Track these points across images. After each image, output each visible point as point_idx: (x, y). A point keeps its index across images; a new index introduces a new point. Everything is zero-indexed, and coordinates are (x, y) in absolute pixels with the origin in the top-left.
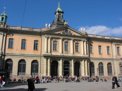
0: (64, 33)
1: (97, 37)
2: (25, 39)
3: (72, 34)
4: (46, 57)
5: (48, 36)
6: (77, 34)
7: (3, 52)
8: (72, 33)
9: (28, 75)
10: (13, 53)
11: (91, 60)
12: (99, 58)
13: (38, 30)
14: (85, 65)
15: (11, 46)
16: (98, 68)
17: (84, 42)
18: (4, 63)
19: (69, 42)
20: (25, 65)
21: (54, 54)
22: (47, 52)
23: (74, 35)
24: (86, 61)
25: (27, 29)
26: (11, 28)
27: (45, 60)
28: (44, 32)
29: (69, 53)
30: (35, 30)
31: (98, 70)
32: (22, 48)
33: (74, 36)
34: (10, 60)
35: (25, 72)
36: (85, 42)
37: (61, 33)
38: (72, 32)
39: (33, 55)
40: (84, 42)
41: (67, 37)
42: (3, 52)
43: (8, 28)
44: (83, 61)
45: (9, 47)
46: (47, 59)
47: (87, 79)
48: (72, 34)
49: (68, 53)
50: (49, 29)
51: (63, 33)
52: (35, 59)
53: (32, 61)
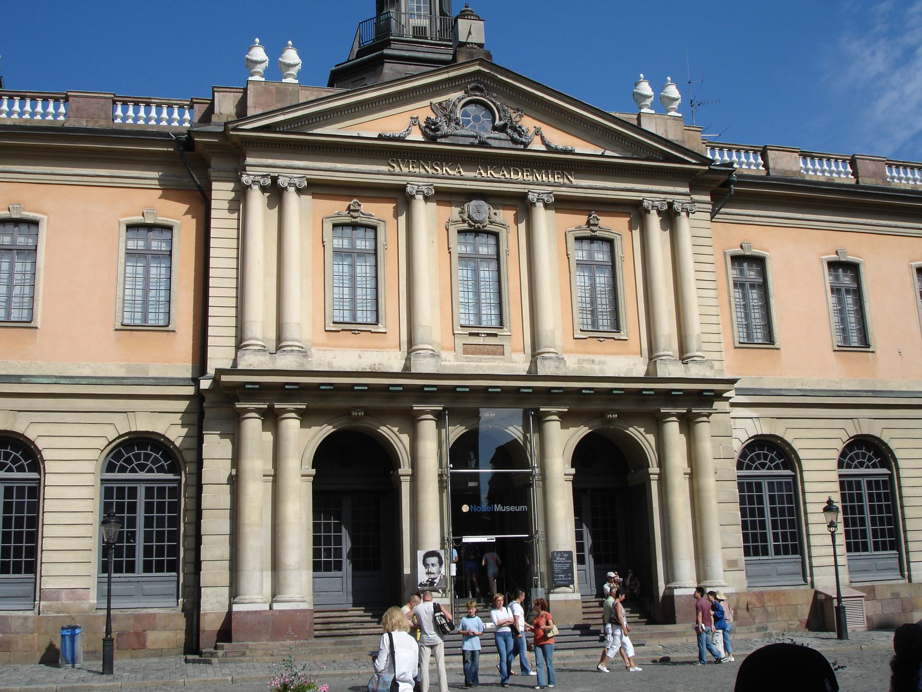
1: (811, 176)
5: (274, 172)
6: (583, 148)
8: (537, 132)
9: (65, 601)
12: (837, 393)
13: (178, 120)
14: (693, 476)
16: (837, 498)
20: (35, 491)
25: (52, 113)
28: (224, 135)
29: (507, 349)
30: (128, 117)
31: (833, 535)
35: (31, 568)
38: (528, 123)
40: (670, 217)
41: (484, 184)
48: (537, 145)
49: (499, 350)
50: (282, 92)
51: (431, 130)
53: (102, 443)
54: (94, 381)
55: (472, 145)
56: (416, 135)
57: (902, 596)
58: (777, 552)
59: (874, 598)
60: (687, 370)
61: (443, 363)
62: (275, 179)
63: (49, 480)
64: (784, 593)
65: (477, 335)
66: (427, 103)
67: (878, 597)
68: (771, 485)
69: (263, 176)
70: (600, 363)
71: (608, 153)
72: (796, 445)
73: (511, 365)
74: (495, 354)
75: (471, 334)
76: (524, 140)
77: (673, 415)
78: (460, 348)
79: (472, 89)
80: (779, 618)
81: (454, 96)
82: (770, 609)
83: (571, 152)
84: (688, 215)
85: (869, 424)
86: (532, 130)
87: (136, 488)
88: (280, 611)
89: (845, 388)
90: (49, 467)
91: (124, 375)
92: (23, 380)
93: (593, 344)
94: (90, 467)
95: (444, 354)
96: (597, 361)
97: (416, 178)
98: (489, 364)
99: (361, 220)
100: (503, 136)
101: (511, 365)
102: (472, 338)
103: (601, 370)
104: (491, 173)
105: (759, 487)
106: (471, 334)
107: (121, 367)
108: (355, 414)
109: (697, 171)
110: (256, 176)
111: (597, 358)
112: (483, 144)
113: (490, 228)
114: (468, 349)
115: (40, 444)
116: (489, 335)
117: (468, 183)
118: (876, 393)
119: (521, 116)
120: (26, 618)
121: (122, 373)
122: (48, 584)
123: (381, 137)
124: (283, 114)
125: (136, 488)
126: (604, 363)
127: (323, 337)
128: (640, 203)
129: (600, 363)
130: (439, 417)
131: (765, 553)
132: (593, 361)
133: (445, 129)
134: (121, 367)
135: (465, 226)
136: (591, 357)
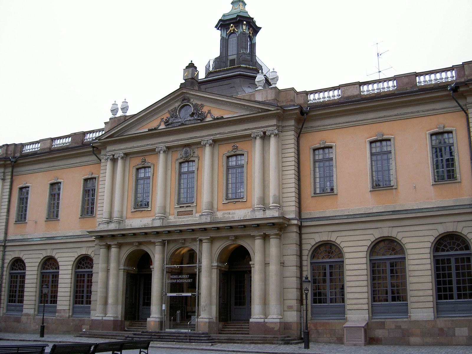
0: (172, 123)
2: (59, 180)
3: (209, 115)
4: (105, 239)
5: (113, 153)
8: (209, 112)
10: (26, 237)
15: (22, 217)
17: (265, 137)
19: (196, 160)
21: (137, 222)
23: (215, 119)
24: (273, 242)
27: (103, 251)
29: (194, 212)
33: (220, 123)
36: (273, 141)
39: (78, 236)
44: (258, 242)
47: (283, 335)
48: (209, 119)
49: (190, 213)
52: (84, 252)
53: (74, 259)
54: (72, 237)
55: (179, 126)
56: (163, 126)
57: (403, 327)
59: (384, 328)
60: (264, 214)
61: (169, 221)
62: (114, 155)
63: (61, 272)
64: (328, 323)
65: (183, 207)
66: (166, 111)
67: (386, 328)
69: (111, 155)
70: (232, 214)
72: (342, 245)
73: (195, 219)
74: (190, 215)
75: (180, 207)
76: (199, 118)
77: (257, 236)
78: (176, 214)
79: (183, 100)
80: (325, 336)
81: (177, 105)
82: (320, 331)
83: (222, 118)
84: (276, 135)
85: (385, 231)
86: (207, 112)
87: (85, 274)
88: (105, 320)
89: (375, 211)
90: (61, 268)
91: (81, 234)
92: (55, 238)
93: (231, 206)
94: (70, 267)
95: (170, 217)
96: (231, 213)
98: (187, 219)
99: (146, 165)
100: (192, 118)
101: (195, 219)
102: (181, 209)
103: (233, 217)
106: (180, 207)
107: (80, 231)
108: (135, 244)
109: (277, 113)
110: (109, 155)
111: (231, 211)
112: (183, 124)
113: (192, 159)
114: (179, 214)
115: (58, 260)
116: (187, 206)
117: (179, 142)
118: (394, 212)
119: (202, 106)
120: (53, 319)
121: (80, 234)
122: (59, 308)
123: (149, 130)
124: (114, 130)
125: (85, 274)
126: (234, 213)
127: (130, 215)
128: (249, 136)
129: (232, 214)
130: (163, 243)
132: (229, 213)
133: (170, 122)
134: (80, 231)
135: (181, 160)
136: (229, 211)
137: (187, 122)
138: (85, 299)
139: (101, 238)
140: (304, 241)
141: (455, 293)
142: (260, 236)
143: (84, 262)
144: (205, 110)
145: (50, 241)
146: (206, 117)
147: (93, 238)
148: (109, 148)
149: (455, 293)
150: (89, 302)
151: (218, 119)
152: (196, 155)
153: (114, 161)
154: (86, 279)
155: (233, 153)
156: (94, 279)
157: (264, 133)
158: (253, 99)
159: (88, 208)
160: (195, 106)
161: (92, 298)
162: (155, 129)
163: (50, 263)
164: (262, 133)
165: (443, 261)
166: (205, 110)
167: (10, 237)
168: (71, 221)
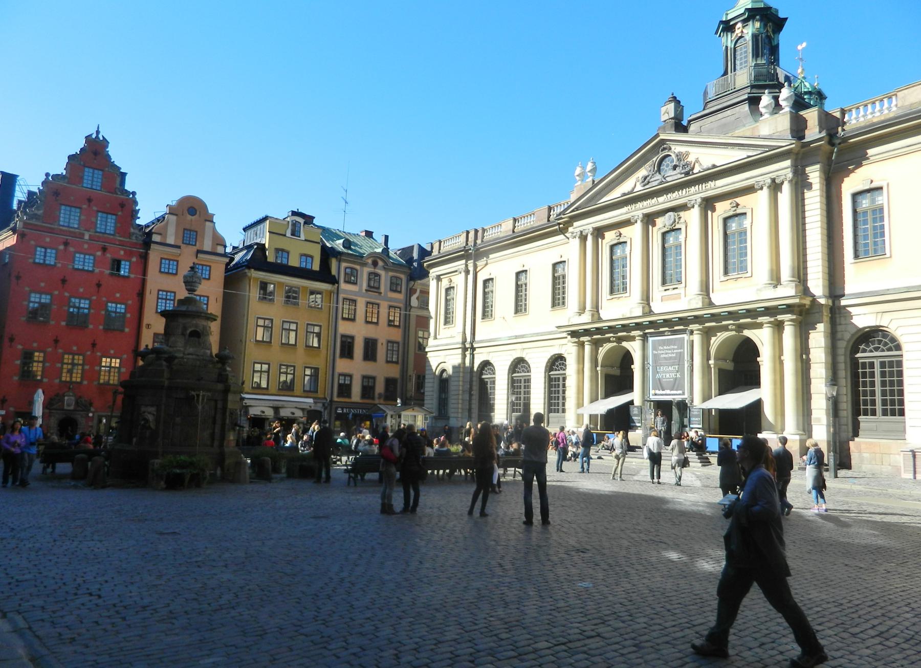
3: (697, 165)
5: (581, 229)
7: (469, 340)
8: (697, 161)
11: (848, 309)
17: (775, 187)
18: (474, 379)
22: (582, 310)
26: (489, 236)
32: (517, 311)
34: (486, 364)
37: (639, 187)
39: (550, 333)
42: (469, 340)
43: (479, 241)
45: (484, 316)
46: (581, 345)
49: (678, 297)
56: (639, 187)
58: (885, 413)
68: (883, 365)
71: (750, 154)
83: (714, 166)
97: (638, 211)
100: (675, 172)
104: (654, 201)
105: (872, 365)
109: (791, 149)
119: (688, 154)
131: (874, 413)
135: (665, 229)
137: (668, 179)
138: (561, 407)
139: (574, 334)
140: (839, 328)
141: (879, 407)
142: (770, 323)
143: (557, 361)
144: (691, 159)
145: (518, 340)
146: (693, 169)
147: (565, 335)
148: (576, 224)
149: (879, 407)
150: (564, 411)
151: (709, 169)
152: (682, 220)
153: (583, 238)
154: (561, 383)
155: (731, 213)
156: (568, 383)
157: (773, 180)
158: (756, 134)
159: (558, 300)
160: (680, 156)
161: (567, 406)
162: (629, 193)
163: (519, 364)
164: (769, 181)
165: (891, 363)
166: (691, 159)
167: (477, 338)
168: (542, 316)
